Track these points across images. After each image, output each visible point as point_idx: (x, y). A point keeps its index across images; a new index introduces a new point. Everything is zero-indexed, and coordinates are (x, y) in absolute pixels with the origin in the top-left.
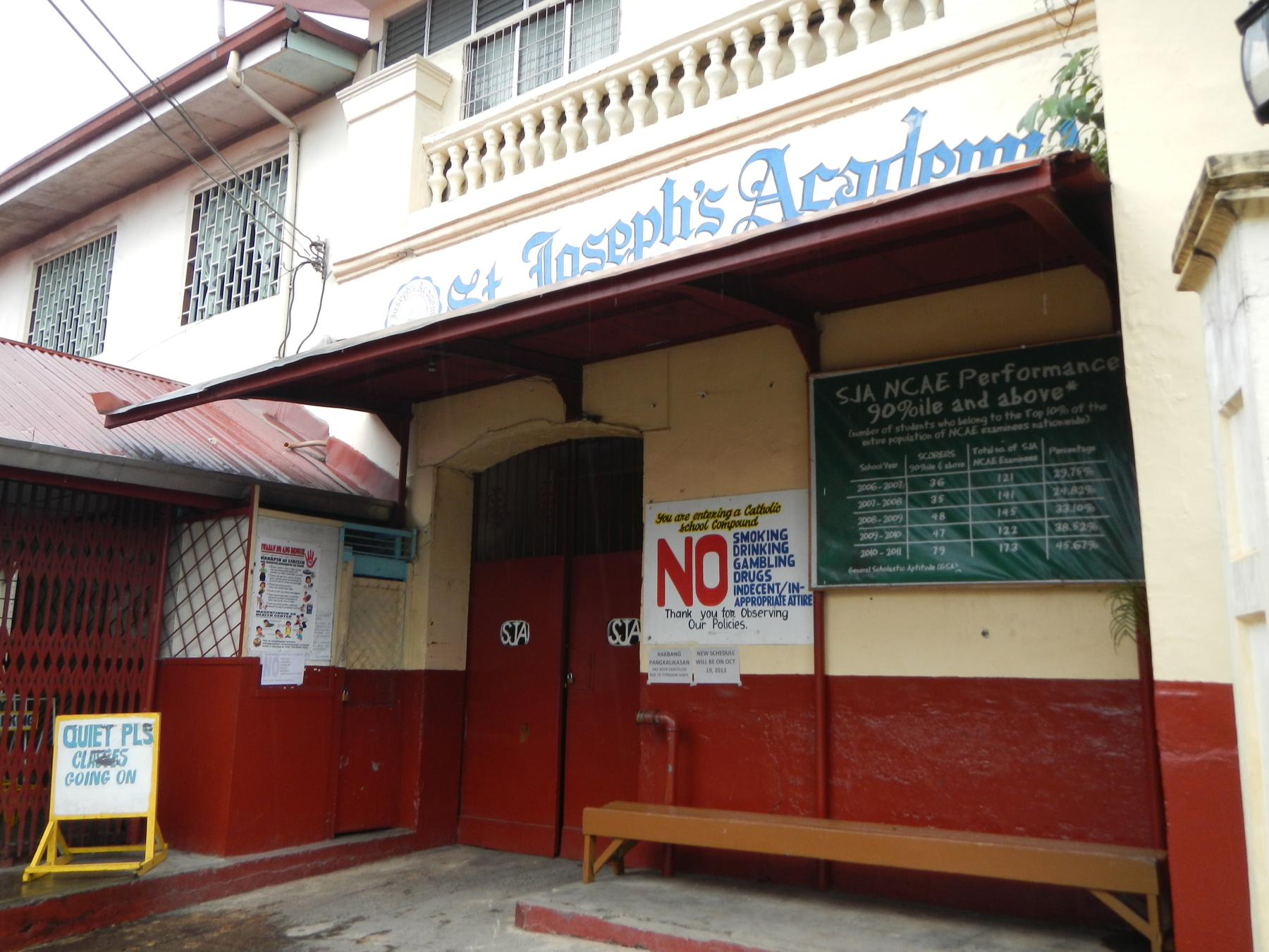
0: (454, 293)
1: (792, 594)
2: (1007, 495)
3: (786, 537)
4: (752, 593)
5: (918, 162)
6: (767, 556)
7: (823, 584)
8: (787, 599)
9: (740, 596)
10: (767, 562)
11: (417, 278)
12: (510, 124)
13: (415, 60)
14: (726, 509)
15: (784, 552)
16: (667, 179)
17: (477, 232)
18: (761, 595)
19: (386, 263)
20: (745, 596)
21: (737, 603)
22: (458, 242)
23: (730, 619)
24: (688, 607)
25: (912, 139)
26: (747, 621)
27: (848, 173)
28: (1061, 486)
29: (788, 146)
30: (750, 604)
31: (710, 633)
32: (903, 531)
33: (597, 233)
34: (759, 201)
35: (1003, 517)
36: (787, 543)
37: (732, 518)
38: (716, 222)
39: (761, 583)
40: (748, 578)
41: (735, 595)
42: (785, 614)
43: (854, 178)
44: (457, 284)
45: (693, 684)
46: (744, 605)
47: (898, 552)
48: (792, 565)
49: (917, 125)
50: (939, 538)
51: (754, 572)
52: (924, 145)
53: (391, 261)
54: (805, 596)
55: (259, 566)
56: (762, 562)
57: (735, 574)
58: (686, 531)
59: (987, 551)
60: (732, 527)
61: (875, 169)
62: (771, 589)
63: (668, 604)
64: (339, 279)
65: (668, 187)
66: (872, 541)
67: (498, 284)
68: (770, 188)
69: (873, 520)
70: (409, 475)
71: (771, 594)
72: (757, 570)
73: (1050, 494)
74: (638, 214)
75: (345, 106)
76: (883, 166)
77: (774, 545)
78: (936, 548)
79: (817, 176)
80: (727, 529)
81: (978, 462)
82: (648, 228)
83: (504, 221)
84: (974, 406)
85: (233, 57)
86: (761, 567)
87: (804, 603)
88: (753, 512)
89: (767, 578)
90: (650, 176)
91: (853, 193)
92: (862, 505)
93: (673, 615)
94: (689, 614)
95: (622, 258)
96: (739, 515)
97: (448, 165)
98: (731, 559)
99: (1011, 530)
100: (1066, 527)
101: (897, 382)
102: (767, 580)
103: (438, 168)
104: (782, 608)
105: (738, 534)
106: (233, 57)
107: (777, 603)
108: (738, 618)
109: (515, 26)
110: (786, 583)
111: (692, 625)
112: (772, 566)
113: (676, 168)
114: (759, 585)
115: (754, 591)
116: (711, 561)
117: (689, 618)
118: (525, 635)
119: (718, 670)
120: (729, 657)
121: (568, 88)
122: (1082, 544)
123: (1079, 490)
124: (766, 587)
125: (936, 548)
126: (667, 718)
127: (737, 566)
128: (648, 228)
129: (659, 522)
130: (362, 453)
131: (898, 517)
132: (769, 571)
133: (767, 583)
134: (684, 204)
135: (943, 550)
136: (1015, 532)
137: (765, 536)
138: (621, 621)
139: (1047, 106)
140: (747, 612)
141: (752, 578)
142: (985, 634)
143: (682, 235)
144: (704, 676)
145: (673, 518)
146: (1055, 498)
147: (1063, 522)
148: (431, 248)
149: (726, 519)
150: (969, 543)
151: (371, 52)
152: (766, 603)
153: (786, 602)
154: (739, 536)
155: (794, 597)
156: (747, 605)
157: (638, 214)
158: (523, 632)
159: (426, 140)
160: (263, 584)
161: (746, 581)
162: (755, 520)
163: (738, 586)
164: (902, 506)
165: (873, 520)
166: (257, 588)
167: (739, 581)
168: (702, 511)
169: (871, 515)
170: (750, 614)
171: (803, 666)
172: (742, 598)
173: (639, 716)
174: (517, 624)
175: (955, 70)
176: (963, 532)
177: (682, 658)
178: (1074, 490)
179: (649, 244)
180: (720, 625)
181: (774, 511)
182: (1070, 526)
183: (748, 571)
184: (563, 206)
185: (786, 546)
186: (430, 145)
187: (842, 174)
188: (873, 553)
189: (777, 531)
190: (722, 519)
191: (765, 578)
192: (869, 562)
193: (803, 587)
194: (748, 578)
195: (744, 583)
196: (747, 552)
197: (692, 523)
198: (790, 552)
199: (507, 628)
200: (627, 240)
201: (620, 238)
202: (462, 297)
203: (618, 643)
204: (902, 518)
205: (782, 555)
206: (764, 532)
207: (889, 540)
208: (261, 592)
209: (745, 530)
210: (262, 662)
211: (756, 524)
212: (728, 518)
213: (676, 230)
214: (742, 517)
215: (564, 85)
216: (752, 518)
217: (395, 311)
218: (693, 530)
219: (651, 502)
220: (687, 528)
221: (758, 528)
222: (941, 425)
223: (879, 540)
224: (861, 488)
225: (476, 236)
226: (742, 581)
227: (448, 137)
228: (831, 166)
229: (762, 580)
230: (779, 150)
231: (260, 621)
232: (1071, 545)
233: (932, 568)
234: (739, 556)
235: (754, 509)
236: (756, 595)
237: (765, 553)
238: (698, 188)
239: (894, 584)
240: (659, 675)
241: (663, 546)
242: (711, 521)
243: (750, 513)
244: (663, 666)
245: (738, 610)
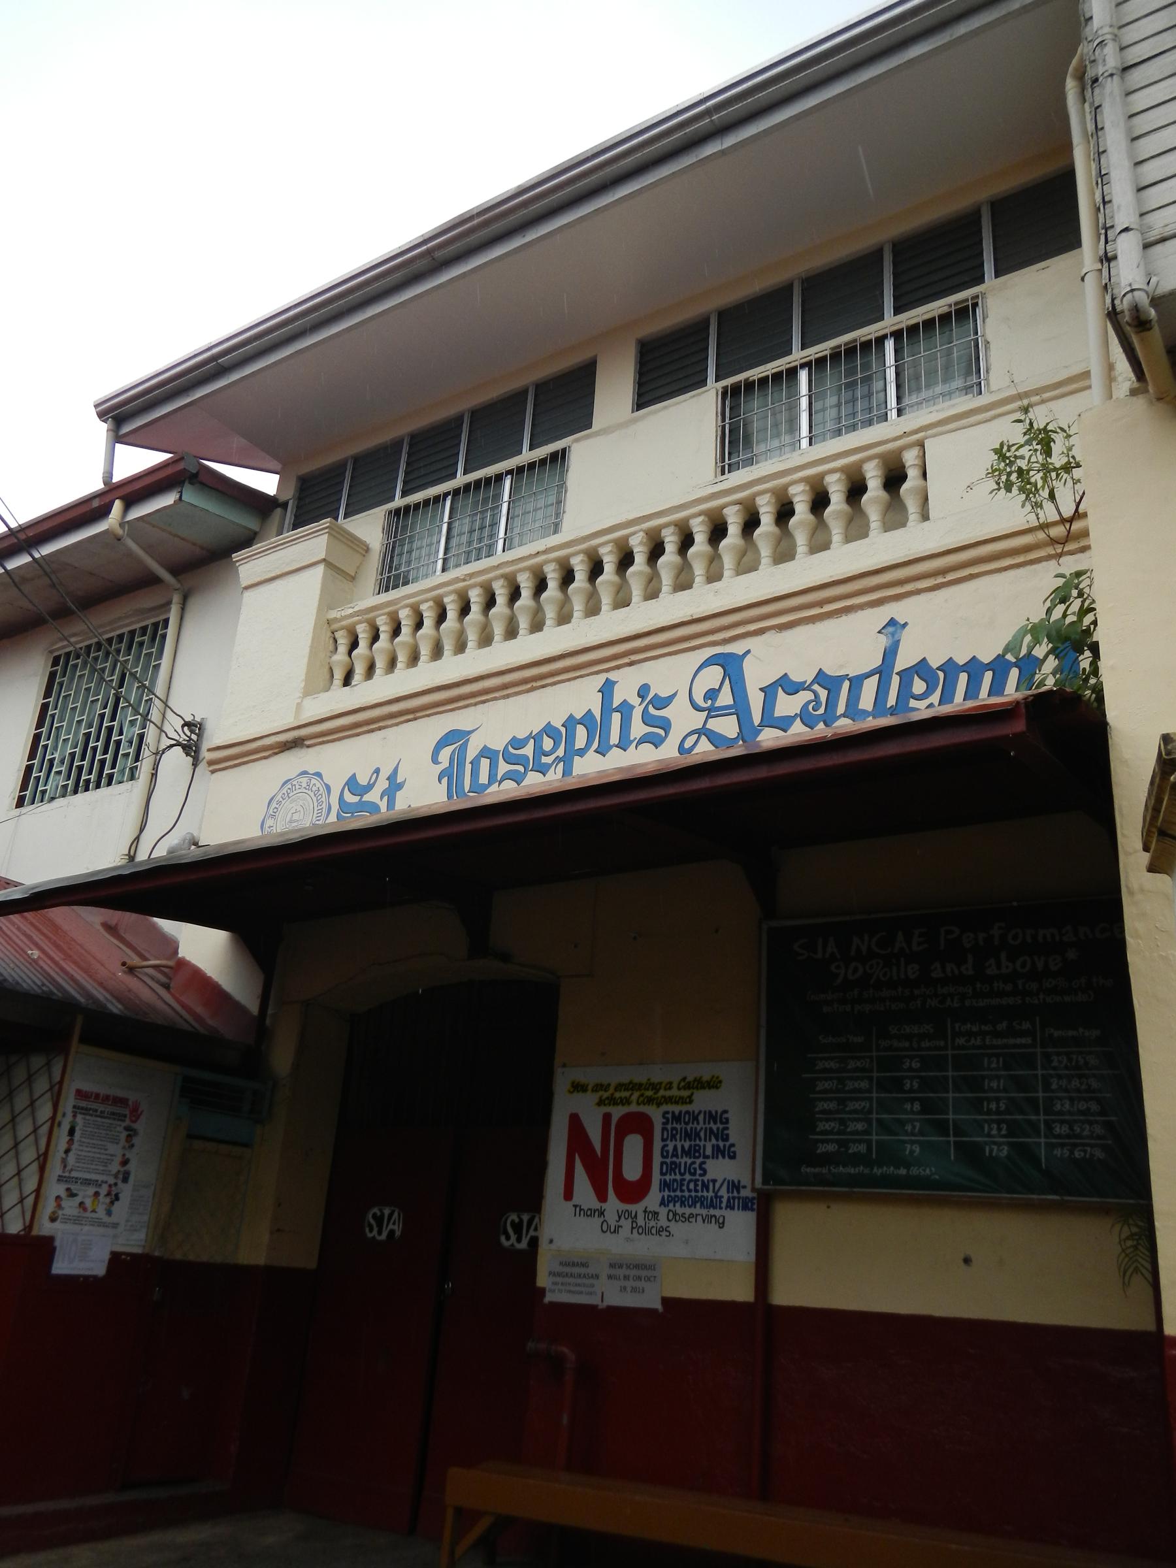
0: (347, 793)
1: (730, 1195)
2: (994, 1084)
3: (727, 1120)
4: (682, 1191)
5: (896, 680)
6: (702, 1144)
7: (769, 1184)
8: (725, 1200)
9: (666, 1193)
10: (702, 1151)
11: (305, 773)
12: (431, 603)
13: (328, 524)
14: (655, 1080)
15: (723, 1140)
16: (607, 679)
17: (381, 724)
18: (693, 1194)
19: (270, 752)
20: (672, 1194)
21: (662, 1203)
22: (358, 735)
23: (652, 1223)
24: (602, 1204)
25: (890, 654)
26: (674, 1227)
27: (816, 687)
28: (1060, 1077)
29: (748, 652)
30: (678, 1205)
31: (627, 1239)
32: (869, 1121)
33: (521, 736)
34: (712, 712)
35: (989, 1112)
36: (727, 1128)
37: (662, 1093)
38: (662, 732)
39: (694, 1178)
40: (677, 1171)
41: (660, 1191)
42: (721, 1221)
43: (823, 694)
44: (352, 784)
45: (602, 1306)
46: (671, 1205)
47: (862, 1148)
48: (733, 1157)
49: (896, 638)
50: (913, 1134)
51: (686, 1163)
52: (903, 661)
53: (276, 751)
54: (747, 1198)
55: (69, 1118)
56: (696, 1151)
57: (662, 1164)
58: (605, 1105)
59: (971, 1154)
60: (662, 1104)
61: (846, 684)
62: (705, 1186)
63: (577, 1199)
64: (212, 768)
65: (607, 690)
66: (831, 1132)
67: (400, 786)
68: (725, 698)
69: (832, 1105)
70: (270, 1012)
71: (705, 1194)
72: (689, 1161)
73: (1047, 1087)
74: (571, 717)
75: (241, 569)
76: (856, 683)
77: (711, 1129)
78: (908, 1146)
79: (780, 688)
80: (654, 1106)
81: (961, 1041)
82: (581, 733)
83: (413, 714)
84: (956, 972)
85: (118, 506)
86: (695, 1157)
87: (745, 1207)
88: (688, 1086)
89: (702, 1172)
90: (588, 675)
91: (821, 711)
92: (820, 1086)
93: (582, 1213)
94: (602, 1213)
95: (549, 766)
96: (670, 1088)
97: (354, 645)
98: (657, 1145)
99: (999, 1129)
100: (1065, 1129)
101: (866, 937)
102: (701, 1175)
103: (343, 649)
104: (717, 1212)
105: (667, 1112)
106: (118, 506)
107: (712, 1206)
108: (663, 1221)
109: (446, 495)
110: (725, 1180)
111: (605, 1228)
112: (708, 1157)
113: (618, 667)
114: (690, 1181)
115: (685, 1188)
116: (633, 1145)
117: (602, 1219)
118: (396, 1227)
119: (634, 1290)
120: (649, 1273)
121: (502, 568)
122: (1085, 1151)
123: (1081, 1084)
124: (700, 1183)
125: (908, 1146)
126: (566, 1350)
127: (665, 1154)
128: (581, 733)
129: (573, 1091)
130: (216, 980)
131: (863, 1104)
132: (704, 1163)
133: (701, 1178)
134: (625, 709)
135: (916, 1148)
136: (1004, 1132)
137: (701, 1118)
138: (519, 1217)
139: (1036, 631)
140: (675, 1214)
141: (682, 1171)
142: (967, 1261)
143: (620, 745)
144: (615, 1296)
145: (590, 1088)
146: (1053, 1091)
147: (1062, 1122)
148: (325, 739)
149: (652, 1092)
150: (949, 1142)
151: (279, 511)
152: (698, 1205)
153: (724, 1205)
154: (670, 1116)
155: (734, 1198)
156: (674, 1206)
157: (571, 717)
158: (394, 1224)
159: (333, 614)
160: (71, 1142)
161: (675, 1174)
162: (690, 1097)
163: (665, 1180)
164: (869, 1091)
165: (832, 1105)
166: (63, 1146)
167: (665, 1174)
168: (625, 1080)
169: (831, 1100)
170: (677, 1218)
171: (741, 1291)
172: (669, 1196)
173: (531, 1345)
175: (940, 580)
176: (941, 1127)
177: (590, 1270)
178: (1075, 1083)
179: (581, 752)
180: (640, 1231)
181: (713, 1087)
182: (1071, 1128)
183: (677, 1161)
184: (484, 702)
185: (726, 1132)
186: (336, 620)
187: (808, 688)
188: (831, 1148)
189: (716, 1112)
190: (650, 1093)
191: (699, 1172)
192: (827, 1160)
193: (744, 1187)
194: (677, 1171)
195: (673, 1177)
196: (678, 1137)
197: (612, 1094)
198: (731, 1141)
199: (374, 1216)
201: (548, 744)
202: (356, 799)
203: (512, 1245)
204: (868, 1105)
205: (721, 1144)
206: (700, 1112)
207: (852, 1133)
208: (67, 1151)
209: (677, 1109)
210: (57, 1243)
211: (691, 1102)
212: (657, 1091)
213: (614, 738)
214: (674, 1092)
215: (496, 564)
216: (685, 1093)
217: (275, 810)
218: (614, 1105)
219: (564, 1066)
220: (606, 1102)
221: (693, 1108)
222: (916, 992)
223: (839, 1133)
224: (820, 1065)
225: (380, 729)
226: (671, 1175)
227: (357, 614)
228: (796, 677)
229: (694, 1174)
230: (738, 655)
231: (60, 1190)
232: (1072, 1152)
233: (903, 1171)
234: (668, 1142)
235: (689, 1083)
236: (686, 1194)
237: (700, 1140)
238: (643, 692)
239: (855, 1190)
240: (560, 1291)
241: (575, 1122)
242: (636, 1094)
243: (685, 1088)
244: (567, 1280)
245: (663, 1211)
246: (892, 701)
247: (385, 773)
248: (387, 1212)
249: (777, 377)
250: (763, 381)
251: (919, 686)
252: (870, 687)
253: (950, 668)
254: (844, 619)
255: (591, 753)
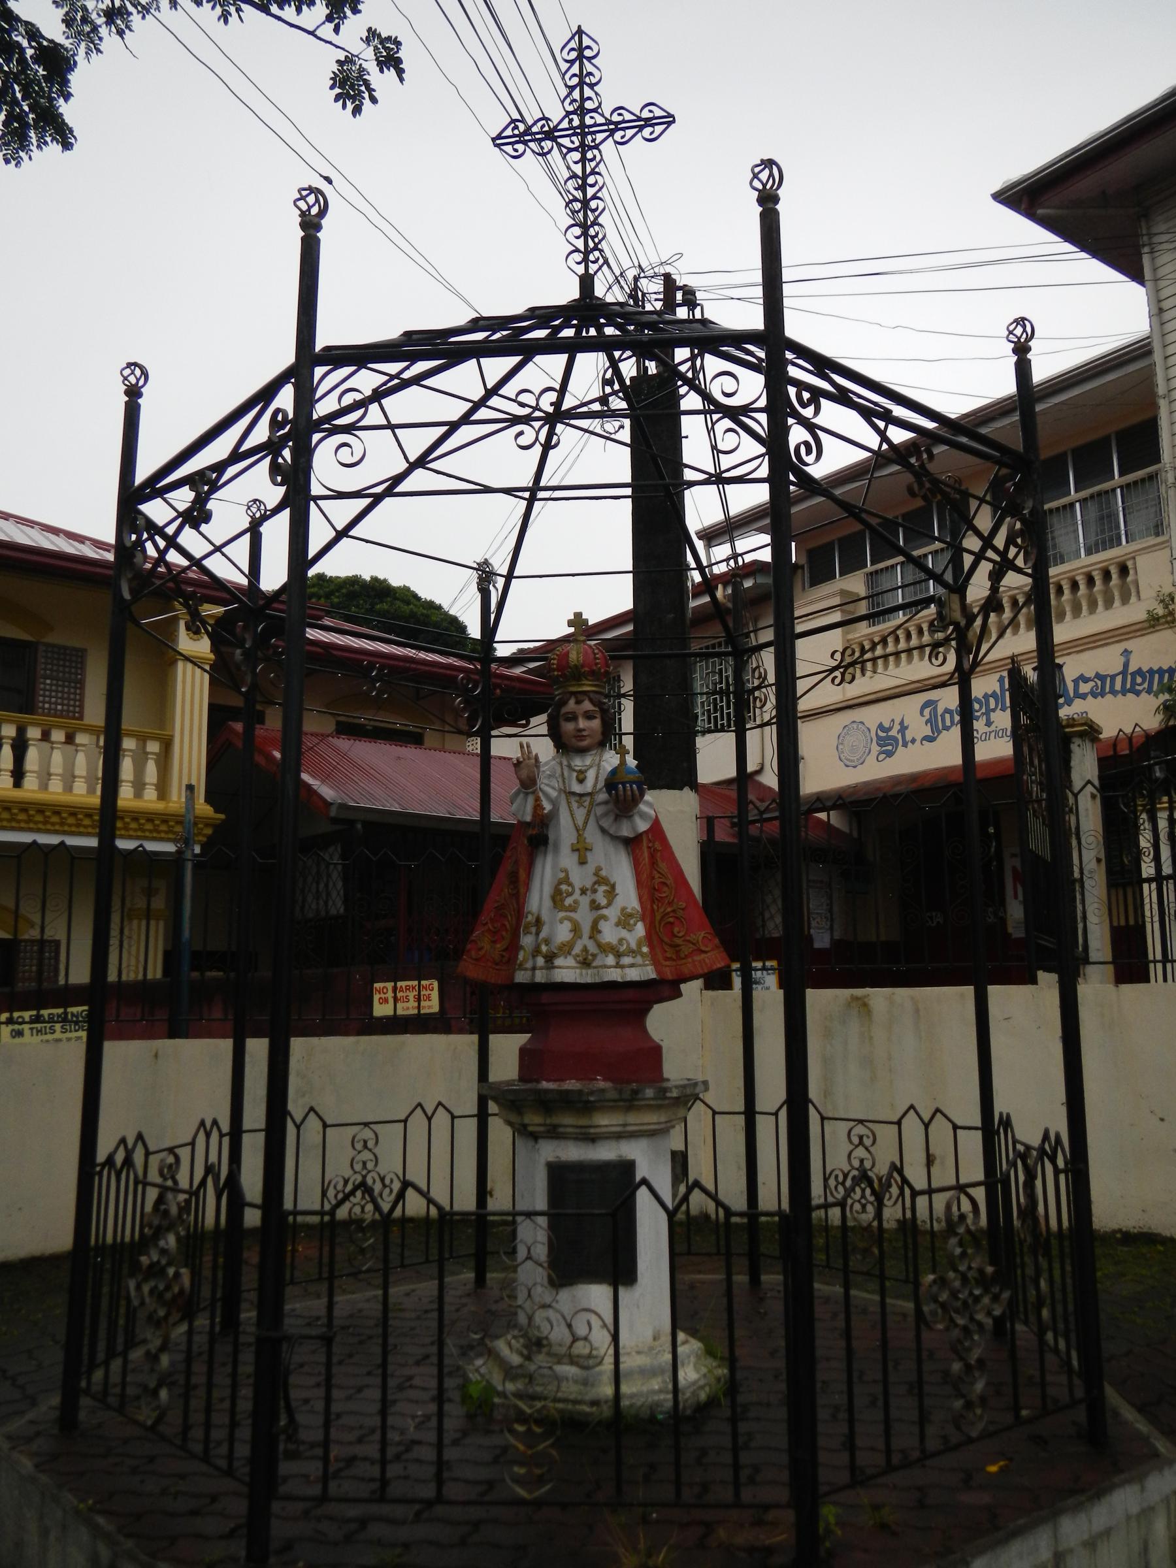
5: (1129, 677)
11: (854, 722)
25: (1126, 665)
43: (1099, 683)
44: (881, 727)
52: (1132, 668)
61: (1109, 679)
67: (907, 728)
74: (986, 694)
76: (1113, 677)
82: (992, 701)
109: (897, 564)
128: (992, 701)
151: (800, 571)
157: (986, 694)
174: (934, 914)
179: (994, 710)
186: (851, 640)
200: (981, 708)
202: (885, 734)
246: (1128, 686)
247: (897, 721)
248: (934, 914)
249: (1064, 507)
250: (1058, 509)
251: (1139, 680)
252: (1119, 679)
253: (1151, 671)
254: (1105, 648)
255: (998, 711)
